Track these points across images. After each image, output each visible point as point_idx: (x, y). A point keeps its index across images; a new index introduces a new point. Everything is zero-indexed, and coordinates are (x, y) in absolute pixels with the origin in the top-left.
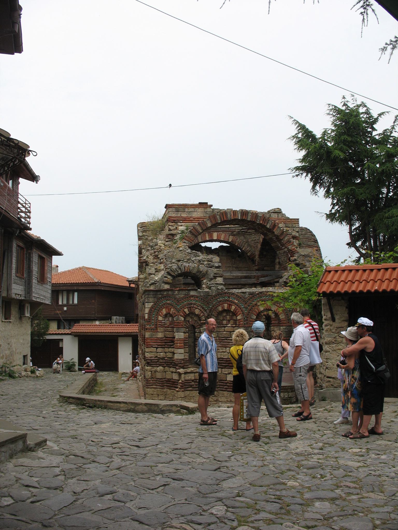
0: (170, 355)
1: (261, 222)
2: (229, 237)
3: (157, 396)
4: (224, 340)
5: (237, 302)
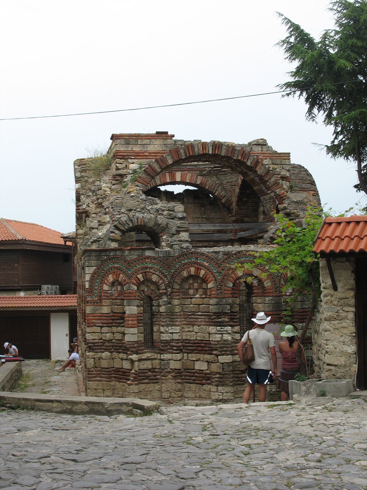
0: (118, 336)
1: (240, 158)
2: (197, 178)
3: (102, 391)
4: (190, 315)
5: (207, 264)
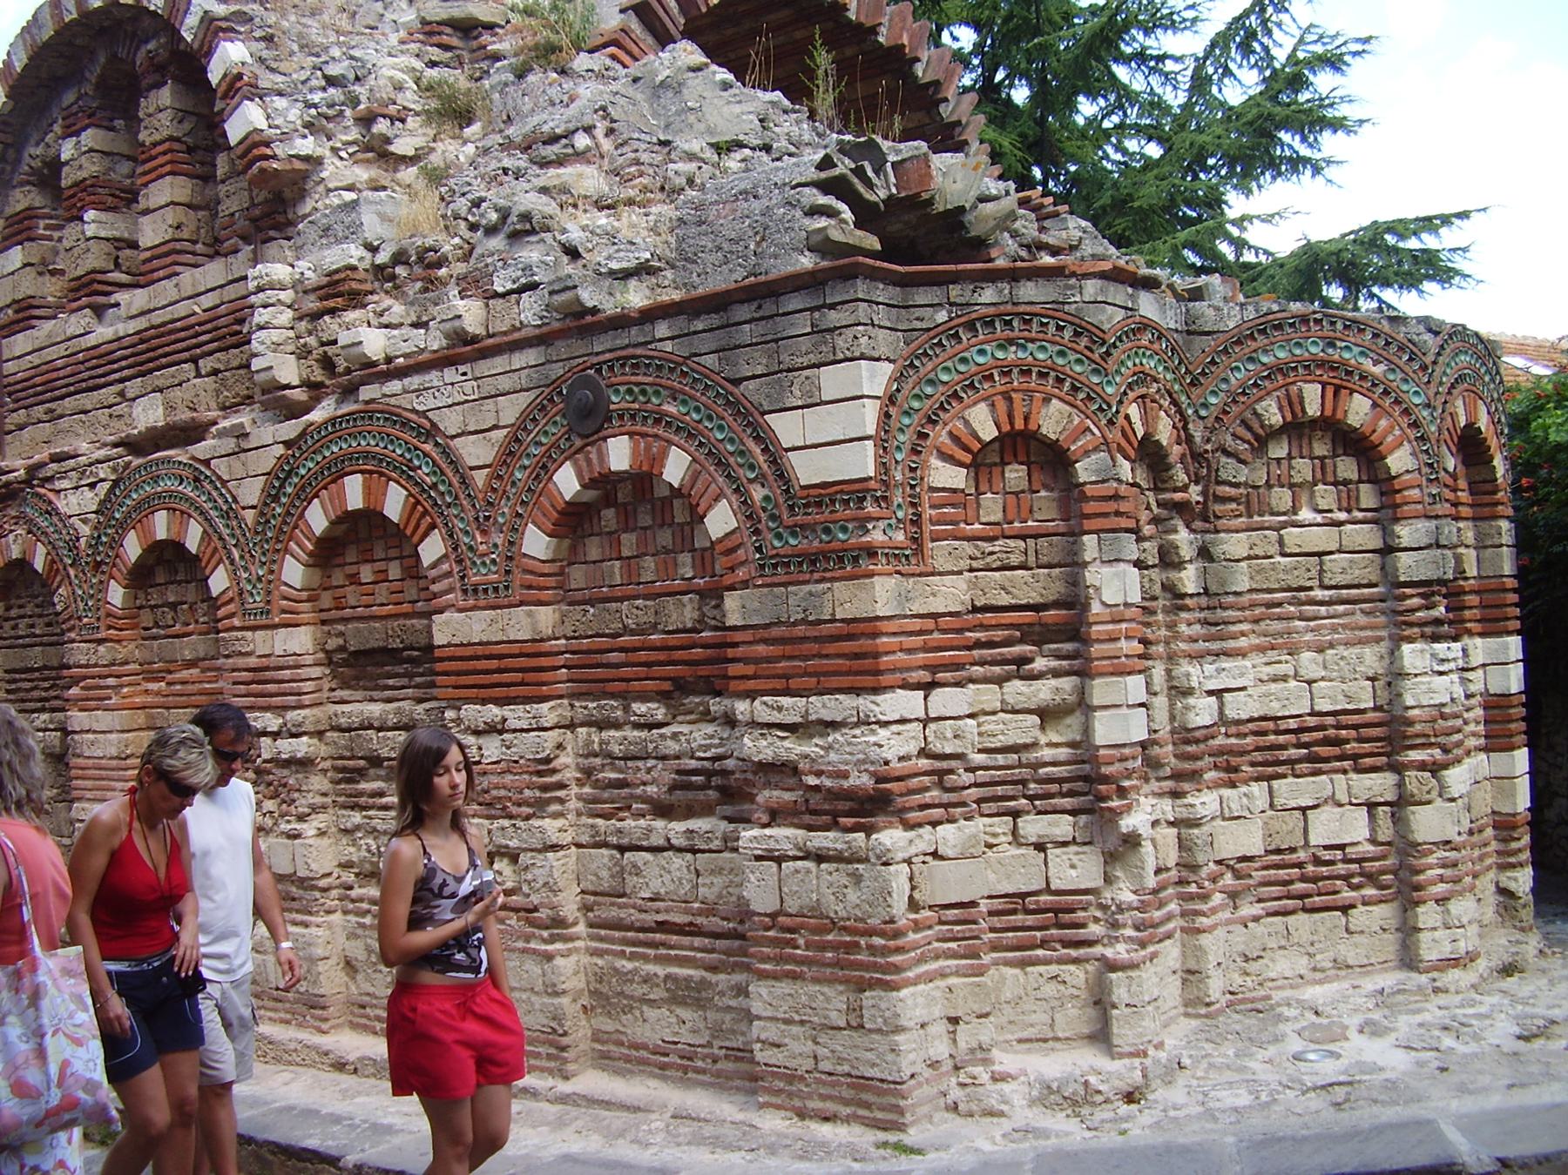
5: (1378, 370)
